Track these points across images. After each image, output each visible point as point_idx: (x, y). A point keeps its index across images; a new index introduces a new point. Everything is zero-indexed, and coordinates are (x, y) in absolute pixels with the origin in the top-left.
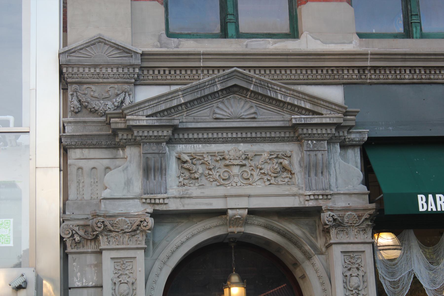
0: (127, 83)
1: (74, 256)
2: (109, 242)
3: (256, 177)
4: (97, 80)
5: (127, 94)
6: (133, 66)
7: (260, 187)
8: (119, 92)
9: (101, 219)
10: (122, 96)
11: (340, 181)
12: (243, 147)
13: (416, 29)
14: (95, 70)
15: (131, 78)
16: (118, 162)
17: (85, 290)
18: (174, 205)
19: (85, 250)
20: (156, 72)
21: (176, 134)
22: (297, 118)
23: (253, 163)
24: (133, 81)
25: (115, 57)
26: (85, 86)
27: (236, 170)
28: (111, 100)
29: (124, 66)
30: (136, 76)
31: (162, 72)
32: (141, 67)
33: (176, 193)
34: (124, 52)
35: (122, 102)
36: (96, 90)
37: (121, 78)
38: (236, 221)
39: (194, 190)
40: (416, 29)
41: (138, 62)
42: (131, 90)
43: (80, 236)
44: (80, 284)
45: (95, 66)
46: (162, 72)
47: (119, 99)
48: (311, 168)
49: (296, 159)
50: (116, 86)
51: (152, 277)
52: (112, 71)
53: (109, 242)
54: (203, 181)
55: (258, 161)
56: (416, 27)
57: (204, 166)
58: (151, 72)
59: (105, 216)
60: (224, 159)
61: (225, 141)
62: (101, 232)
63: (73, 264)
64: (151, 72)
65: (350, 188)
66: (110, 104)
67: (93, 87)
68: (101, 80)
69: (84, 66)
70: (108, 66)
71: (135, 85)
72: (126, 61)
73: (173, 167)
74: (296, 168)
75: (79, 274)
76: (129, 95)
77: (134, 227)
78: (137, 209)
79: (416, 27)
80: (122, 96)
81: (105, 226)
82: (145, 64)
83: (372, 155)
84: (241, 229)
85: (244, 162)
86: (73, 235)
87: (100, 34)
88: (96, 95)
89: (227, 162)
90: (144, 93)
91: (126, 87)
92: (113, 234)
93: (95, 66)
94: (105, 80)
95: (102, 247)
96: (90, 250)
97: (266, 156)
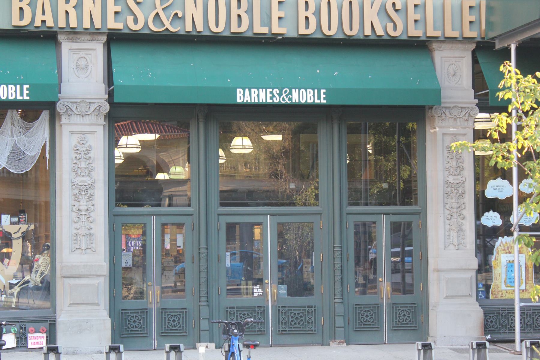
83: (117, 54)
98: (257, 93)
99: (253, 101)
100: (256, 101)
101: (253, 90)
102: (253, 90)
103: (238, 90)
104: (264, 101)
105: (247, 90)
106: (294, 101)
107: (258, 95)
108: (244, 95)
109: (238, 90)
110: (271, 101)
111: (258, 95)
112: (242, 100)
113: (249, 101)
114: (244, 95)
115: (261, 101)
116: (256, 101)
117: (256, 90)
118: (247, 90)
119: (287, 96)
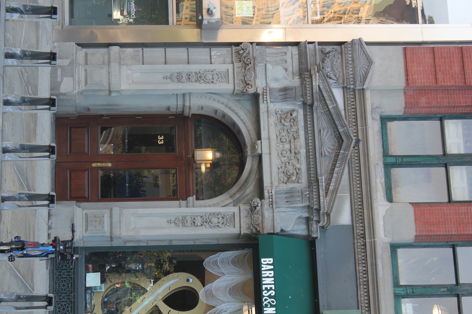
0: (344, 81)
1: (230, 51)
2: (238, 68)
3: (283, 159)
4: (344, 63)
5: (336, 81)
6: (355, 84)
7: (276, 162)
8: (337, 76)
9: (252, 62)
10: (335, 79)
11: (282, 214)
12: (303, 151)
13: (402, 291)
14: (350, 61)
15: (347, 84)
16: (291, 76)
17: (209, 58)
18: (262, 107)
19: (234, 57)
20: (352, 100)
21: (308, 107)
22: (323, 184)
23: (292, 158)
24: (345, 85)
25: (360, 72)
26: (340, 56)
27: (287, 146)
28: (331, 70)
29: (354, 78)
30: (348, 86)
31: (352, 103)
32: (355, 90)
33: (270, 109)
34: (364, 78)
35: (330, 78)
36: (337, 62)
37: (347, 78)
38: (254, 147)
39: (273, 120)
40: (402, 291)
41: (358, 88)
42: (339, 84)
43: (242, 54)
44: (212, 55)
45: (353, 60)
46: (352, 103)
47: (332, 76)
48: (290, 194)
49: (296, 185)
50: (341, 75)
51: (217, 98)
52: (351, 71)
53: (238, 68)
54: (280, 127)
55: (294, 161)
56: (403, 290)
57: (289, 127)
58: (352, 96)
59: (254, 64)
60: (295, 139)
61: (306, 139)
62: (244, 62)
63: (225, 50)
64: (352, 96)
65: (277, 220)
66: (329, 69)
67: (339, 61)
68: (344, 65)
69: (352, 51)
70: (354, 68)
71: (343, 88)
72: (358, 79)
73: (287, 107)
74: (290, 186)
75: (219, 54)
76: (336, 83)
77: (248, 82)
78: (259, 85)
79: (403, 290)
80: (335, 79)
81: (248, 65)
82: (357, 92)
84: (249, 153)
85: (293, 151)
86: (243, 49)
87: (374, 62)
88: (335, 63)
89: (292, 140)
90: (338, 94)
91: (341, 81)
92: (243, 70)
93: (353, 60)
94: (344, 68)
95: (235, 64)
96: (234, 59)
97: (298, 166)
98: (270, 276)
99: (263, 272)
100: (263, 275)
101: (272, 272)
102: (272, 272)
103: (272, 259)
104: (263, 283)
105: (272, 267)
106: (265, 309)
107: (268, 277)
108: (268, 264)
109: (272, 259)
110: (264, 289)
111: (268, 277)
112: (263, 262)
113: (263, 269)
114: (268, 264)
115: (263, 279)
116: (263, 275)
117: (272, 275)
118: (272, 267)
119: (269, 302)
